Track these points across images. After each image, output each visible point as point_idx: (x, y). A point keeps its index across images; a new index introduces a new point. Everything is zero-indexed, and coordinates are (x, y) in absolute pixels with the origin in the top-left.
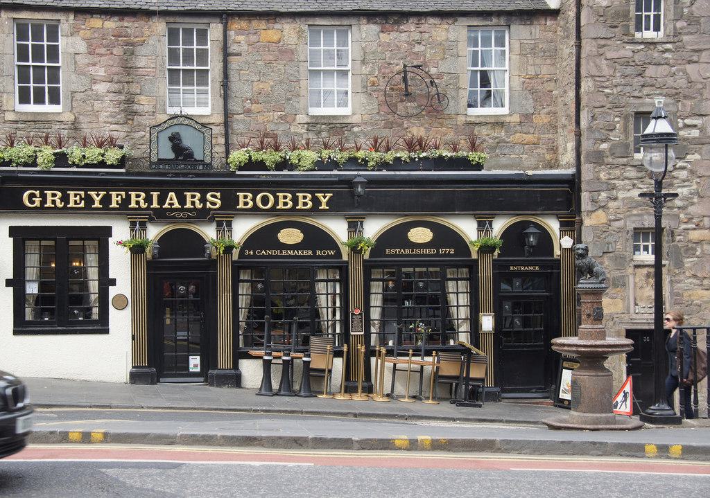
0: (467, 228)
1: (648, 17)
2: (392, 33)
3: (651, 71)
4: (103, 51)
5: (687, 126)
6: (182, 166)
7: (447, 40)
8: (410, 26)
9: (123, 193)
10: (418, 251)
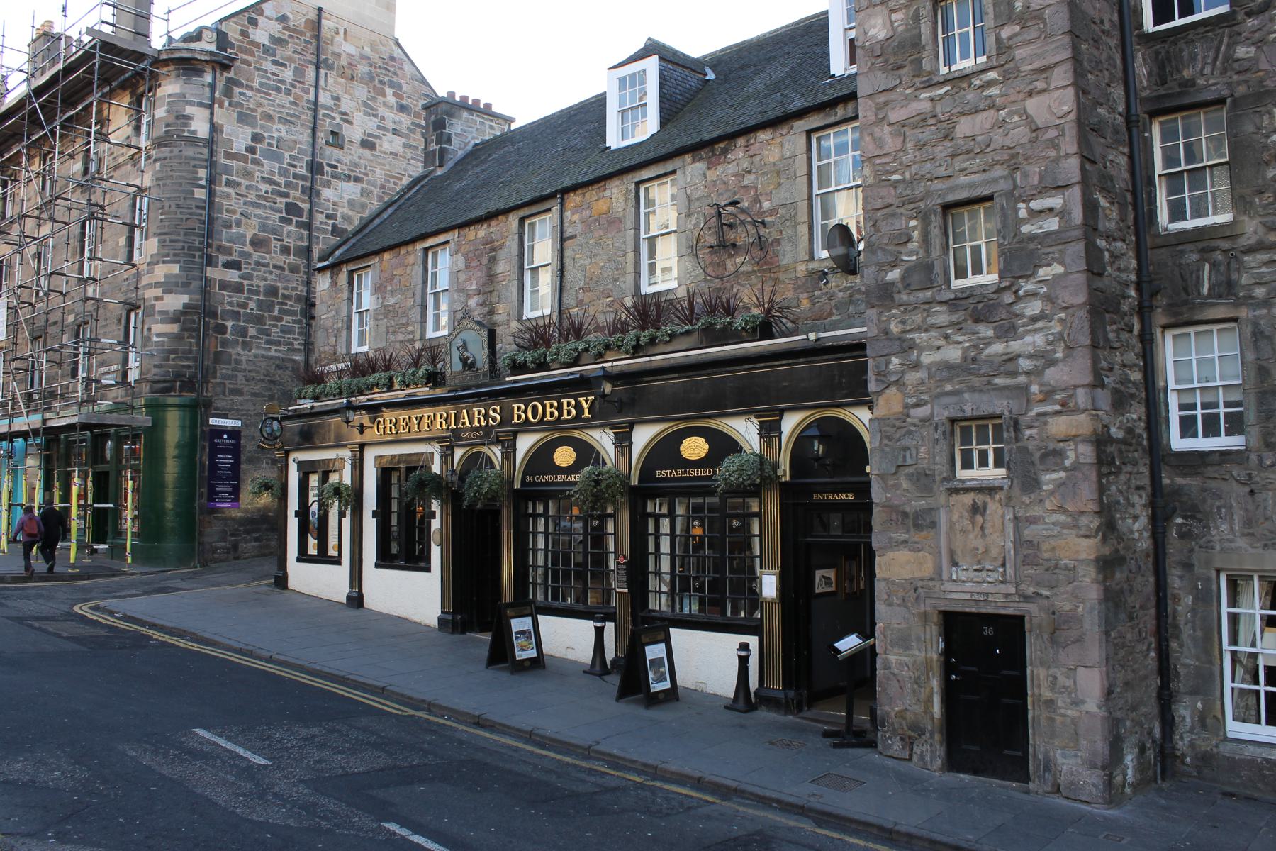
0: (745, 430)
1: (964, 37)
3: (965, 127)
4: (474, 263)
5: (1035, 214)
7: (782, 158)
8: (739, 152)
10: (693, 473)
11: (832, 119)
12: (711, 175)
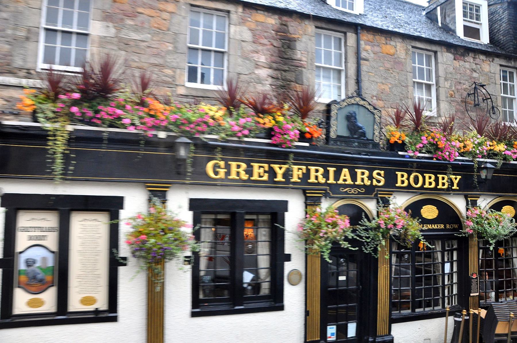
2: (460, 61)
6: (356, 144)
9: (304, 167)
11: (510, 65)
12: (456, 63)
